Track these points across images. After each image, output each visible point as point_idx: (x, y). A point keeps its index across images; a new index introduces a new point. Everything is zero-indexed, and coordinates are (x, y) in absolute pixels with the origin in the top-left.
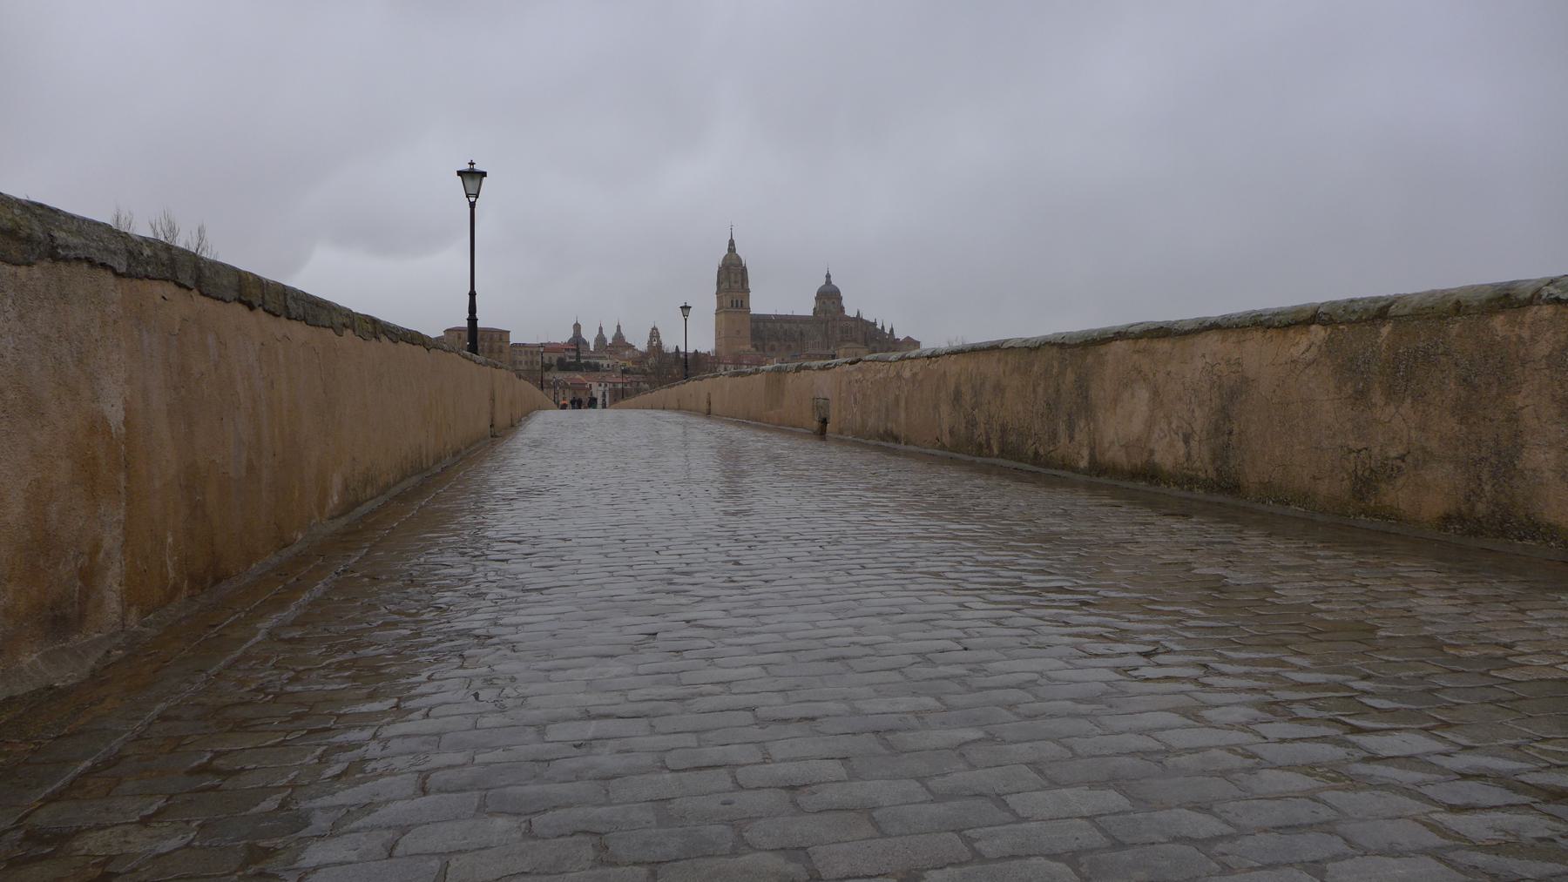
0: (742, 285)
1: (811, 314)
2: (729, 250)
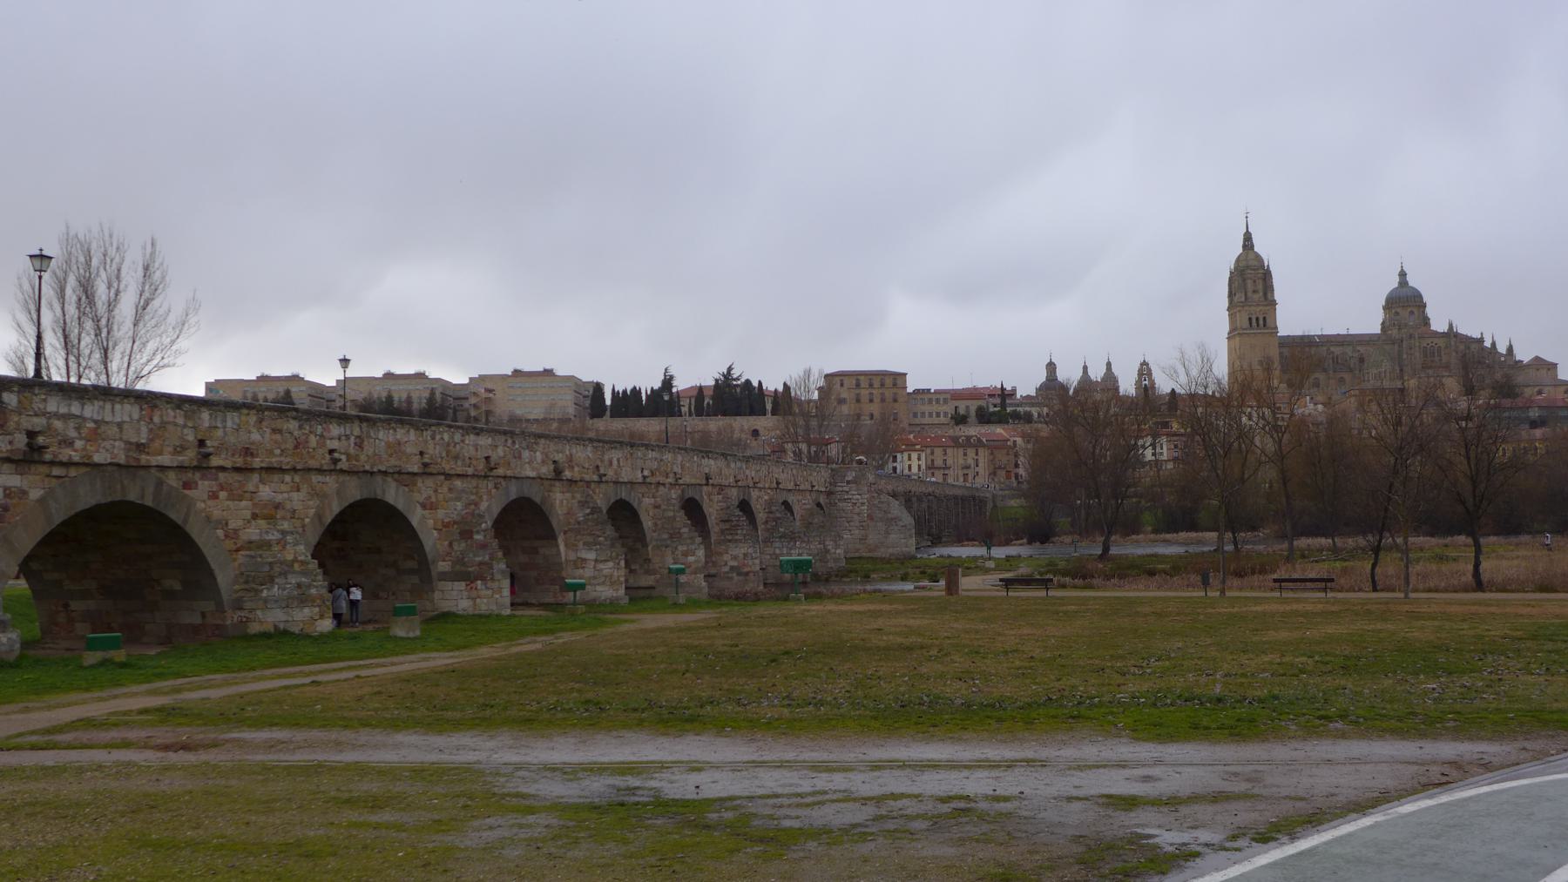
0: (1265, 294)
1: (1377, 330)
2: (1244, 246)
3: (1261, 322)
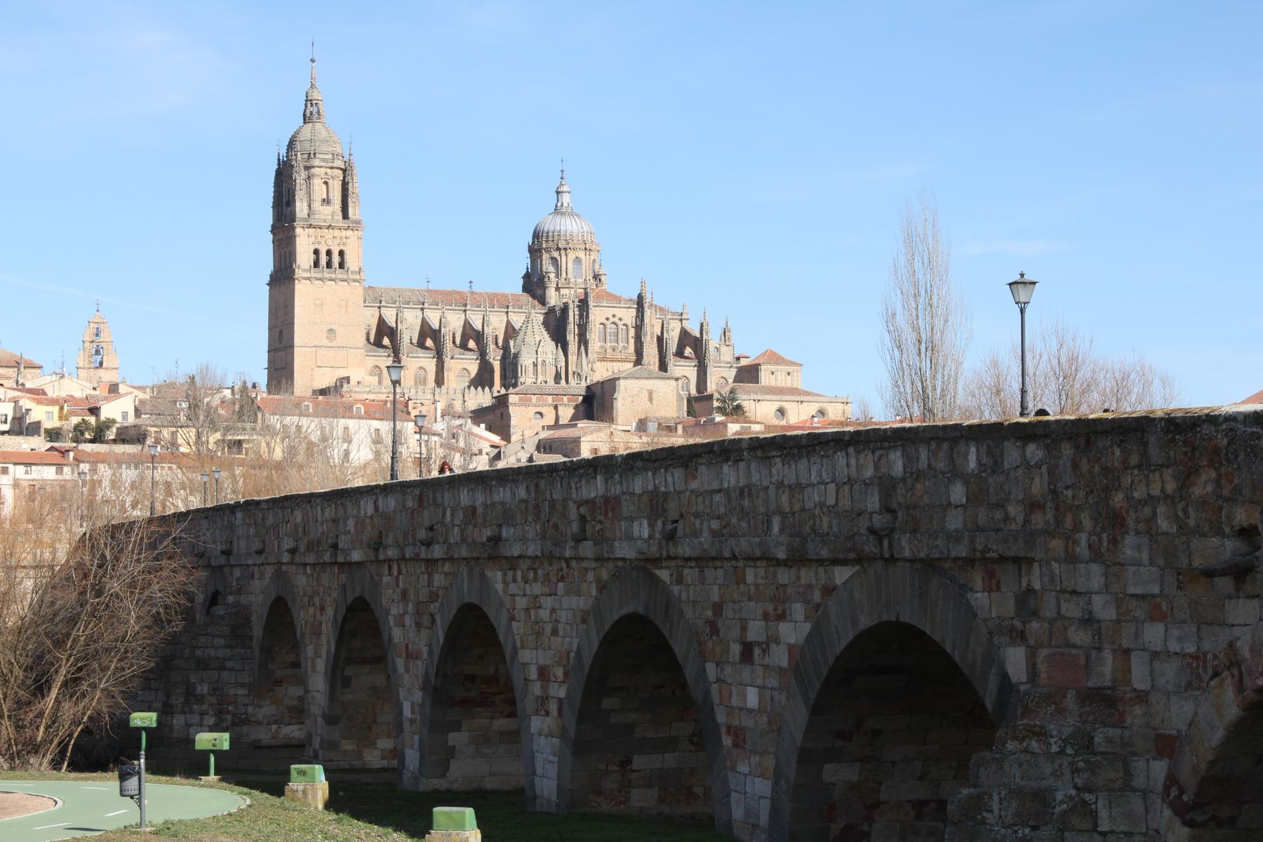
3: (336, 259)
